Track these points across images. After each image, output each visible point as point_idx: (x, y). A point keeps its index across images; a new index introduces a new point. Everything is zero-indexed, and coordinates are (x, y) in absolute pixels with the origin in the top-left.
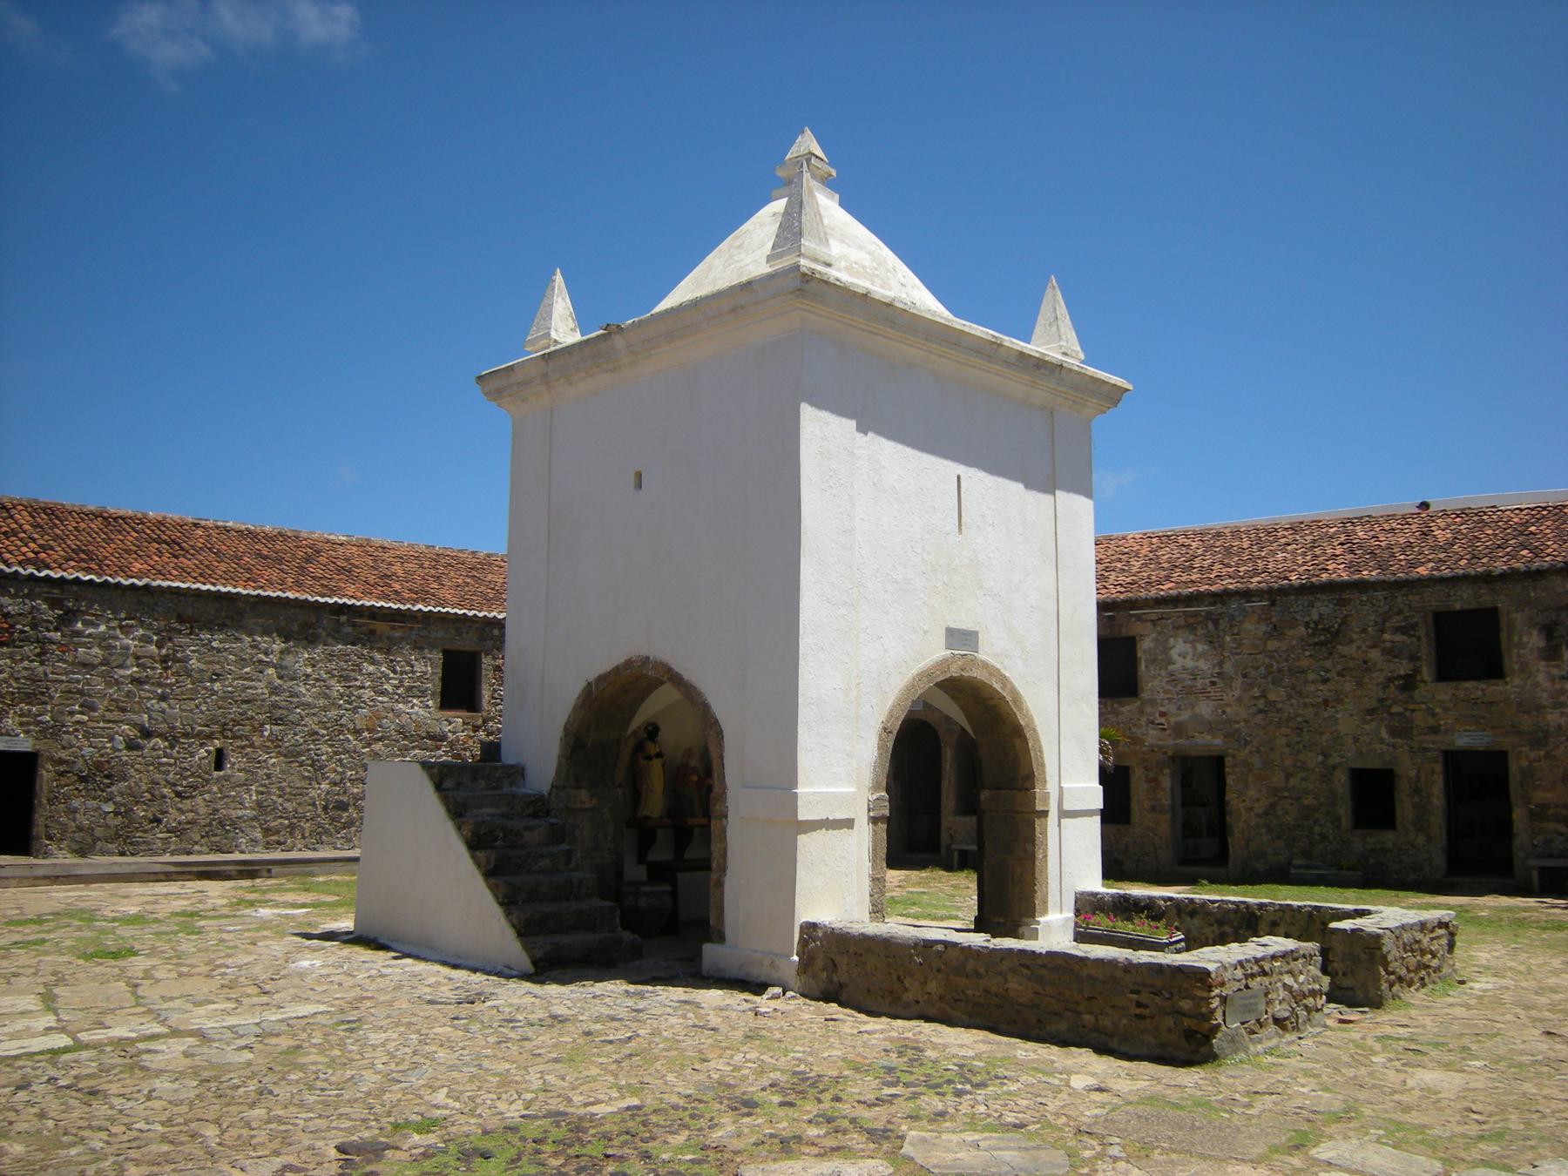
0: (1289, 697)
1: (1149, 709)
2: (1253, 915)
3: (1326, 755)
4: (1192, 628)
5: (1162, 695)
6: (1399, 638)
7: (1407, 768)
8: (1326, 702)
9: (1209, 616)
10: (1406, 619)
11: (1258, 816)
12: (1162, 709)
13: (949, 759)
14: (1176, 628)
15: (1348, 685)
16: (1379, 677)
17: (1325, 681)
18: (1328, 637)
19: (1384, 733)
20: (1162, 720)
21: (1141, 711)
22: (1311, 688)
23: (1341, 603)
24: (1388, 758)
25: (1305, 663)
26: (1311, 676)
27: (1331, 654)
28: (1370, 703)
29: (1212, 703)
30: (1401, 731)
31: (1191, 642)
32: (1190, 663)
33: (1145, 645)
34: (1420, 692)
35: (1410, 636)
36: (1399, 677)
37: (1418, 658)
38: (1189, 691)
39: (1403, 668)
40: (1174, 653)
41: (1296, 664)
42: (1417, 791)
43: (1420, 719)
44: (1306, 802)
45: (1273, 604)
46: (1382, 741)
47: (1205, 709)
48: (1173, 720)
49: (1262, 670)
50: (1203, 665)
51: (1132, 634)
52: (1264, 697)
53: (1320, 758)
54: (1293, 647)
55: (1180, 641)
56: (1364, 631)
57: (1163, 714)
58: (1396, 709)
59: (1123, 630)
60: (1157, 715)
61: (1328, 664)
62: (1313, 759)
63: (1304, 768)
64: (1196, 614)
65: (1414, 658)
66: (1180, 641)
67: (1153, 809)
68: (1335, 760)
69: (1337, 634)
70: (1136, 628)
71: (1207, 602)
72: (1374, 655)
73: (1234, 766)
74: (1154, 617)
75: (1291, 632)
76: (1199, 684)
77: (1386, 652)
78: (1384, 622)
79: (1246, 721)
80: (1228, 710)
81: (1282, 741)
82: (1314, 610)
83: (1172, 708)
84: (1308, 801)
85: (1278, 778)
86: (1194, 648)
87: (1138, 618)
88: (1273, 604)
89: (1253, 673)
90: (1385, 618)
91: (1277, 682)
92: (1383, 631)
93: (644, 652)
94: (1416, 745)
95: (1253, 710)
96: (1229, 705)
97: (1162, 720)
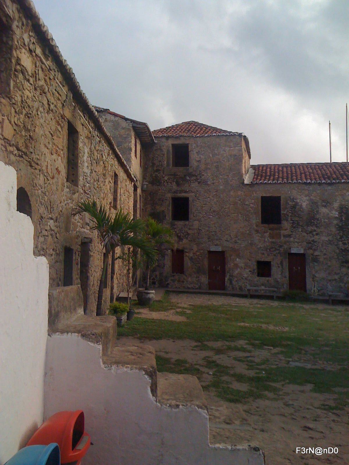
16: (109, 201)
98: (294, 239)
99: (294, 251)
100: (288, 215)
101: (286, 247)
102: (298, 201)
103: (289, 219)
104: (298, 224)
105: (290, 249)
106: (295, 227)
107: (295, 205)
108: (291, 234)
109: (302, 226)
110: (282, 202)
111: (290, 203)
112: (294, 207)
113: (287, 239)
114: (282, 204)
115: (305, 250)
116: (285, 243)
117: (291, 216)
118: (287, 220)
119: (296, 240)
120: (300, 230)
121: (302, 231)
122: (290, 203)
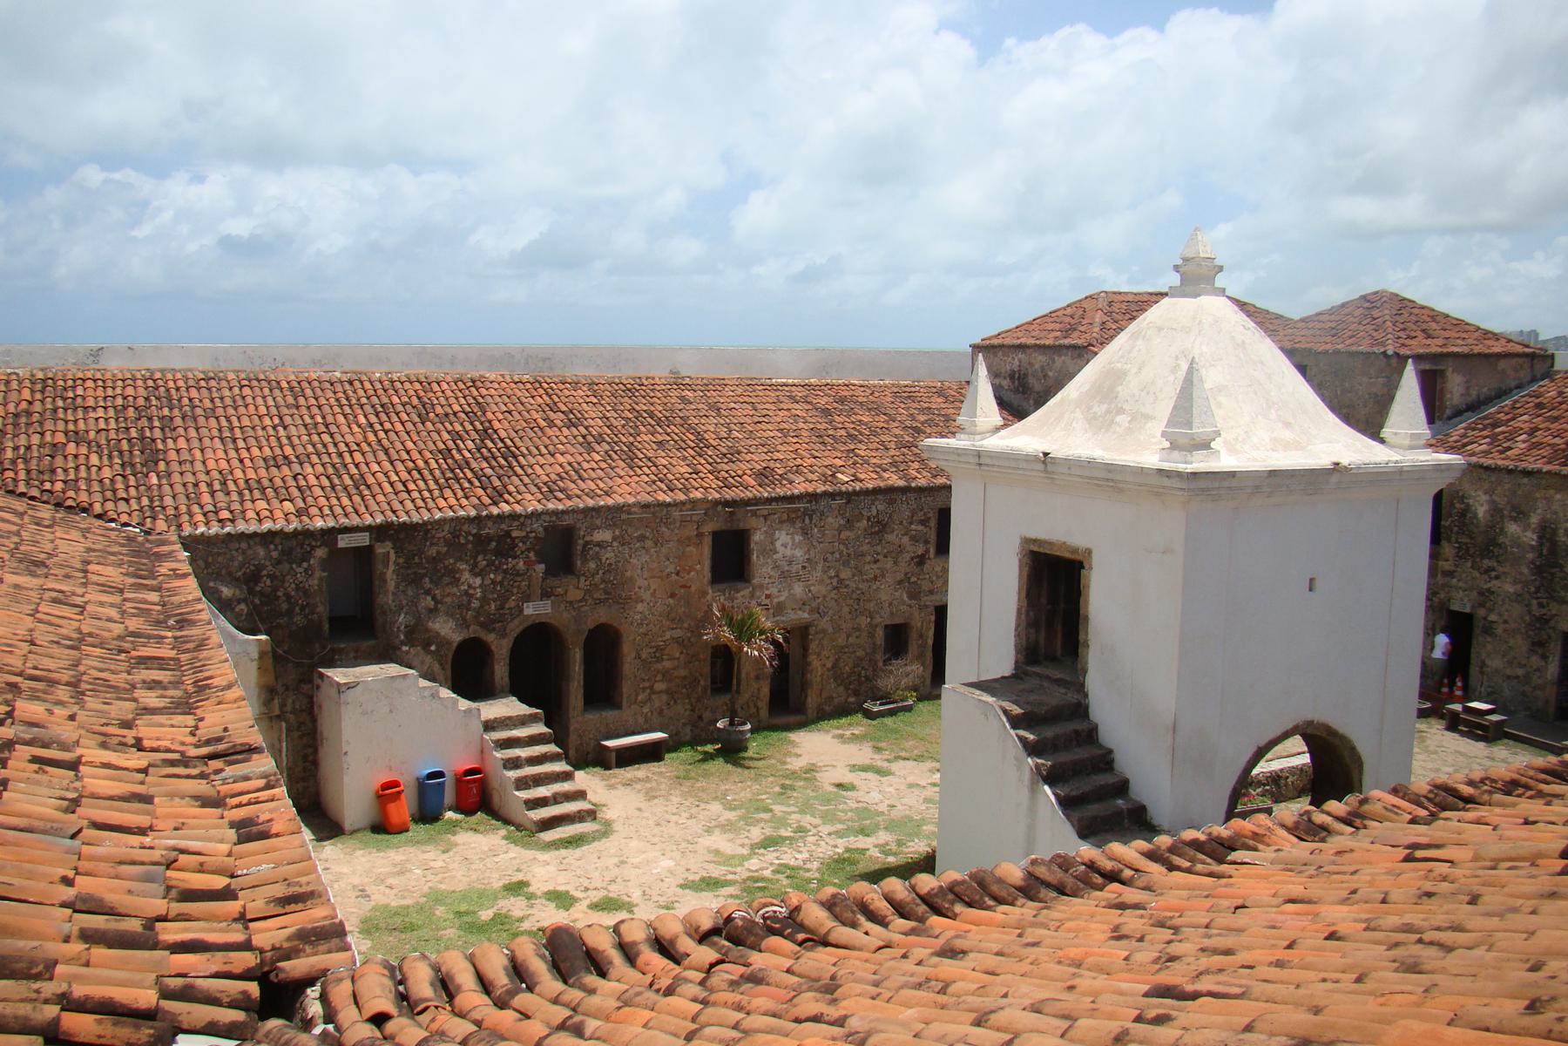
0: (854, 576)
1: (758, 593)
2: (1278, 776)
3: (872, 619)
4: (791, 521)
5: (767, 580)
6: (920, 528)
7: (917, 623)
8: (875, 577)
9: (806, 512)
10: (925, 514)
11: (829, 670)
12: (767, 592)
13: (578, 660)
14: (781, 522)
15: (889, 564)
16: (907, 556)
17: (876, 561)
18: (880, 528)
19: (905, 598)
20: (767, 602)
21: (752, 596)
22: (867, 567)
23: (891, 502)
24: (907, 615)
25: (865, 548)
26: (868, 558)
27: (880, 541)
28: (900, 576)
29: (801, 584)
30: (914, 595)
31: (791, 534)
32: (788, 552)
33: (757, 537)
34: (927, 567)
35: (926, 527)
36: (918, 556)
37: (928, 543)
38: (785, 576)
39: (920, 550)
40: (778, 544)
41: (861, 549)
42: (921, 636)
43: (926, 586)
44: (858, 654)
45: (849, 502)
46: (904, 603)
47: (798, 589)
48: (776, 600)
49: (837, 556)
50: (798, 553)
51: (741, 526)
52: (837, 576)
53: (869, 620)
54: (859, 537)
55: (784, 533)
56: (901, 523)
57: (768, 596)
58: (914, 579)
59: (741, 524)
60: (763, 597)
61: (879, 548)
62: (864, 621)
63: (858, 629)
64: (798, 509)
65: (926, 542)
66: (784, 533)
67: (757, 678)
68: (878, 620)
69: (884, 526)
70: (752, 522)
71: (805, 500)
72: (905, 540)
73: (817, 633)
74: (766, 513)
75: (857, 525)
76: (795, 568)
77: (914, 539)
78: (913, 516)
79: (825, 597)
80: (812, 588)
81: (846, 610)
82: (874, 507)
83: (773, 591)
84: (860, 653)
85: (841, 641)
86: (793, 538)
87: (754, 513)
88: (849, 502)
89: (830, 557)
90: (913, 513)
91: (846, 563)
92: (911, 523)
93: (1309, 717)
94: (922, 604)
95: (829, 588)
96: (813, 585)
97: (767, 602)
98: (1459, 581)
99: (1455, 607)
100: (1451, 531)
101: (1442, 595)
102: (1471, 501)
103: (1453, 539)
104: (1467, 549)
105: (1449, 600)
106: (1461, 558)
107: (1464, 510)
108: (1454, 571)
109: (1472, 557)
110: (1444, 501)
111: (1457, 505)
112: (1463, 514)
113: (1447, 579)
114: (1444, 505)
115: (1473, 607)
116: (1444, 585)
117: (1458, 533)
118: (1449, 541)
119: (1461, 584)
120: (1469, 564)
121: (1472, 567)
122: (1457, 505)
